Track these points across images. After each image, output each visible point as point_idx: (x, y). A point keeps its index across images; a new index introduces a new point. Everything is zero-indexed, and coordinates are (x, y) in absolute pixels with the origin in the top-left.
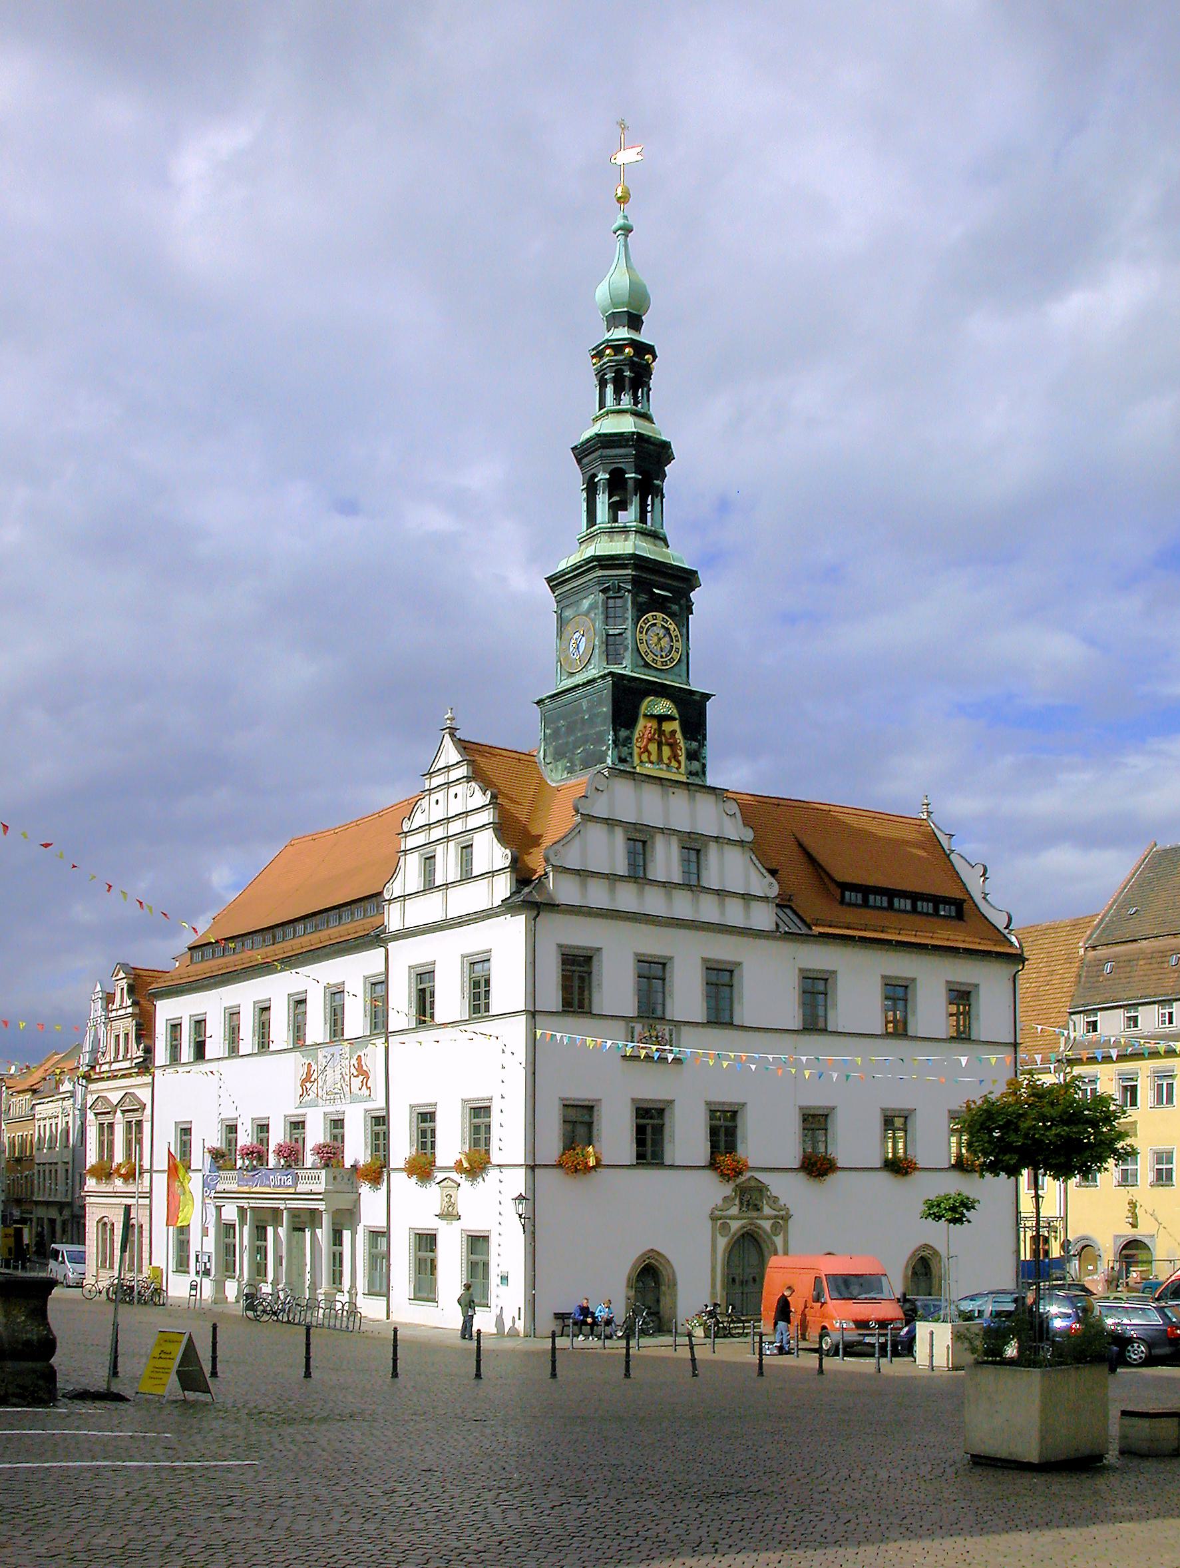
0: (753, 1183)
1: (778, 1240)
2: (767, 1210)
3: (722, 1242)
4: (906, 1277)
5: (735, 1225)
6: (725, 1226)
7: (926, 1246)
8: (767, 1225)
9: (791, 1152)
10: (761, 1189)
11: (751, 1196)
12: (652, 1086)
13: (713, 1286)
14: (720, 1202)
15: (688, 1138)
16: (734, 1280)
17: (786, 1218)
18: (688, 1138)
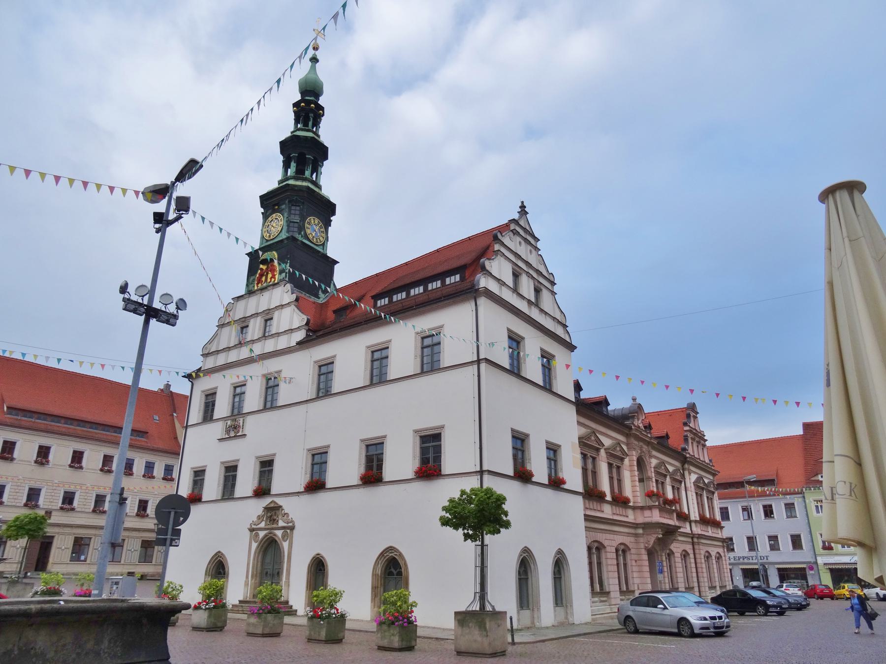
0: (272, 505)
1: (285, 545)
2: (281, 523)
3: (255, 545)
4: (374, 575)
5: (262, 534)
6: (257, 535)
7: (391, 549)
8: (279, 533)
9: (300, 481)
10: (279, 508)
11: (273, 512)
12: (232, 451)
13: (247, 577)
14: (255, 519)
15: (246, 482)
16: (267, 573)
17: (292, 528)
18: (246, 482)
